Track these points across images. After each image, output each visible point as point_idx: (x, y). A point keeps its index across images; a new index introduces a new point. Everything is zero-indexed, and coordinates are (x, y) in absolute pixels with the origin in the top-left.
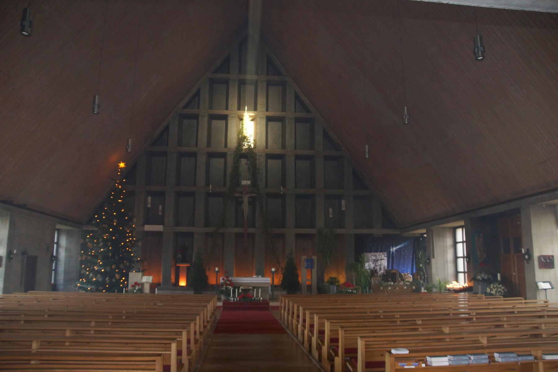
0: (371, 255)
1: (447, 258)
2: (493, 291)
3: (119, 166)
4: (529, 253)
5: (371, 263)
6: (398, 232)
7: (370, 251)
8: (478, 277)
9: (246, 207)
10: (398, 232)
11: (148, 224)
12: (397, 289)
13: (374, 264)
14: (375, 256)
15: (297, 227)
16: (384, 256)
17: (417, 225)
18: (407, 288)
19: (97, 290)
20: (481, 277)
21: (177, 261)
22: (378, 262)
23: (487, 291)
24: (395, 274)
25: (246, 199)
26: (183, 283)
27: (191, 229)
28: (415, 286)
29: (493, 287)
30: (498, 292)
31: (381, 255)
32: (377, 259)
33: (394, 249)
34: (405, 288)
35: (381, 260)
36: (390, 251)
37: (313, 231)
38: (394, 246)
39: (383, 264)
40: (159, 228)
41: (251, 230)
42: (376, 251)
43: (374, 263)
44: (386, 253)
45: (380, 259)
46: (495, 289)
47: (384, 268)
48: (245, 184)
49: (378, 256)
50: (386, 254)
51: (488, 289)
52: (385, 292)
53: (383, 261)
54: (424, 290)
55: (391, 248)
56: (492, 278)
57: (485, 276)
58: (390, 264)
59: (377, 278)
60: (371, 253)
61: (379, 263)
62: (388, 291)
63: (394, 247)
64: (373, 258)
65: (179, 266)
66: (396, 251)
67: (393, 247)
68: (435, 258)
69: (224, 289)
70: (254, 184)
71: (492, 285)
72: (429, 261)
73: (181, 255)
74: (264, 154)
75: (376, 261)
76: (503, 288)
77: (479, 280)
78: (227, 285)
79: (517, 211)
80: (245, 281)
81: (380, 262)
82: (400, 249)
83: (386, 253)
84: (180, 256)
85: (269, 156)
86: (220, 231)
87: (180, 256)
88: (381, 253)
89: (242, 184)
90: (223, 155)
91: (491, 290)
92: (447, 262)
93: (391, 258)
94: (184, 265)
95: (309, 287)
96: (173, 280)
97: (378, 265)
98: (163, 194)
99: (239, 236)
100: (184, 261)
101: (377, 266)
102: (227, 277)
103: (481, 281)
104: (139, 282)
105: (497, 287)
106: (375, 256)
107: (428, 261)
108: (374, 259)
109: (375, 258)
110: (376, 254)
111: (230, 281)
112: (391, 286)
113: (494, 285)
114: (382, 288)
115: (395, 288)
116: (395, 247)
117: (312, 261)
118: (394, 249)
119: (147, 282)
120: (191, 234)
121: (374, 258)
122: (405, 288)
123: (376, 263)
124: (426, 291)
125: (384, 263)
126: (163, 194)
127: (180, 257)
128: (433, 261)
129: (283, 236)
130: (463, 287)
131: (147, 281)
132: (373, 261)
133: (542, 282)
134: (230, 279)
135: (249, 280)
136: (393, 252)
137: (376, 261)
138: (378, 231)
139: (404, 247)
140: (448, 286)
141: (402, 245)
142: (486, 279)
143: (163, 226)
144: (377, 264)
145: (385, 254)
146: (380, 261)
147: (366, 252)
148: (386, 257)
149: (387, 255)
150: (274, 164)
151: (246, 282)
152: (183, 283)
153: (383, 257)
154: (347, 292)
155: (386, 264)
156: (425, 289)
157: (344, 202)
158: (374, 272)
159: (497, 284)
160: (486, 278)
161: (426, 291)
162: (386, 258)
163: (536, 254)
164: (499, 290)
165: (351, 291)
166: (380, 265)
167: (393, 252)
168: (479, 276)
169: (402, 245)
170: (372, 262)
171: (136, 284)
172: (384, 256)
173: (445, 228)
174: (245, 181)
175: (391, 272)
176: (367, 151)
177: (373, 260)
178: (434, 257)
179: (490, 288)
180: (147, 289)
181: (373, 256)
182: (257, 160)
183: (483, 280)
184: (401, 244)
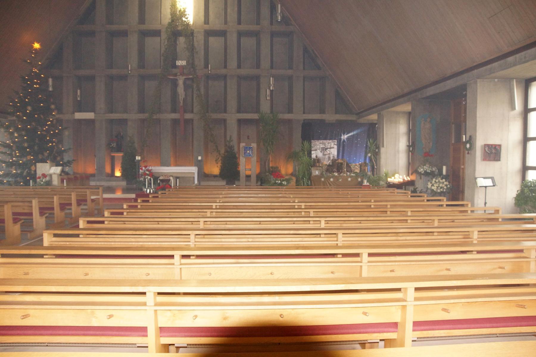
0: (319, 142)
1: (399, 148)
2: (434, 186)
3: (33, 47)
4: (471, 140)
5: (319, 151)
6: (353, 118)
7: (319, 139)
8: (420, 169)
9: (181, 90)
10: (353, 118)
11: (80, 111)
12: (340, 180)
13: (323, 152)
14: (323, 143)
15: (239, 111)
16: (334, 144)
17: (370, 109)
18: (351, 180)
19: (17, 183)
20: (424, 170)
21: (112, 150)
22: (327, 150)
23: (428, 186)
24: (342, 164)
25: (181, 82)
26: (118, 174)
27: (124, 116)
28: (360, 178)
29: (435, 181)
30: (439, 188)
31: (330, 143)
32: (326, 147)
33: (346, 136)
34: (349, 179)
35: (330, 148)
36: (341, 139)
37: (255, 116)
38: (346, 133)
39: (332, 153)
40: (90, 115)
41: (188, 116)
42: (325, 139)
43: (323, 151)
44: (336, 141)
45: (329, 147)
46: (436, 184)
47: (334, 157)
48: (179, 65)
49: (327, 144)
50: (336, 142)
51: (429, 183)
52: (327, 185)
53: (332, 150)
54: (367, 183)
55: (342, 135)
56: (437, 171)
57: (428, 169)
58: (341, 154)
59: (318, 168)
60: (319, 141)
61: (328, 152)
62: (330, 182)
63: (345, 134)
64: (322, 147)
65: (114, 156)
66: (348, 139)
67: (344, 134)
68: (385, 146)
69: (143, 179)
70: (191, 64)
71: (434, 180)
72: (378, 150)
73: (115, 144)
74: (203, 30)
75: (324, 149)
76: (445, 183)
77: (420, 174)
78: (146, 174)
79: (463, 88)
80: (167, 170)
81: (329, 151)
83: (336, 141)
84: (114, 145)
85: (209, 33)
86: (155, 117)
87: (114, 145)
88: (331, 141)
89: (177, 65)
90: (157, 33)
91: (433, 185)
92: (398, 152)
93: (341, 146)
94: (120, 155)
95: (248, 177)
96: (108, 170)
98: (92, 78)
99: (175, 122)
100: (119, 150)
101: (326, 155)
102: (146, 167)
103: (423, 174)
104: (46, 173)
105: (439, 182)
106: (324, 144)
107: (377, 150)
108: (323, 147)
109: (324, 146)
110: (325, 141)
111: (148, 170)
112: (334, 177)
113: (436, 179)
114: (323, 179)
115: (338, 180)
116: (347, 134)
118: (346, 136)
119: (54, 173)
120: (123, 122)
121: (322, 146)
122: (349, 179)
123: (324, 152)
124: (368, 184)
125: (334, 152)
126: (92, 78)
127: (114, 146)
128: (383, 150)
130: (404, 180)
131: (55, 172)
132: (321, 149)
133: (483, 178)
134: (150, 168)
135: (172, 170)
136: (344, 141)
138: (330, 117)
139: (357, 134)
140: (389, 180)
141: (355, 132)
142: (428, 172)
143: (95, 113)
144: (325, 153)
145: (335, 142)
146: (329, 150)
147: (313, 139)
148: (335, 145)
150: (215, 43)
151: (168, 171)
152: (118, 174)
154: (275, 183)
155: (336, 153)
156: (367, 182)
157: (272, 79)
158: (316, 161)
159: (440, 179)
160: (429, 171)
161: (368, 184)
162: (336, 147)
163: (480, 142)
164: (441, 185)
165: (279, 182)
166: (329, 154)
167: (344, 141)
168: (422, 168)
169: (355, 132)
170: (321, 151)
171: (44, 176)
172: (334, 144)
173: (398, 113)
174: (180, 61)
175: (337, 162)
176: (279, 12)
177: (322, 148)
178: (383, 146)
179: (431, 183)
180: (56, 181)
183: (426, 174)
184: (354, 131)
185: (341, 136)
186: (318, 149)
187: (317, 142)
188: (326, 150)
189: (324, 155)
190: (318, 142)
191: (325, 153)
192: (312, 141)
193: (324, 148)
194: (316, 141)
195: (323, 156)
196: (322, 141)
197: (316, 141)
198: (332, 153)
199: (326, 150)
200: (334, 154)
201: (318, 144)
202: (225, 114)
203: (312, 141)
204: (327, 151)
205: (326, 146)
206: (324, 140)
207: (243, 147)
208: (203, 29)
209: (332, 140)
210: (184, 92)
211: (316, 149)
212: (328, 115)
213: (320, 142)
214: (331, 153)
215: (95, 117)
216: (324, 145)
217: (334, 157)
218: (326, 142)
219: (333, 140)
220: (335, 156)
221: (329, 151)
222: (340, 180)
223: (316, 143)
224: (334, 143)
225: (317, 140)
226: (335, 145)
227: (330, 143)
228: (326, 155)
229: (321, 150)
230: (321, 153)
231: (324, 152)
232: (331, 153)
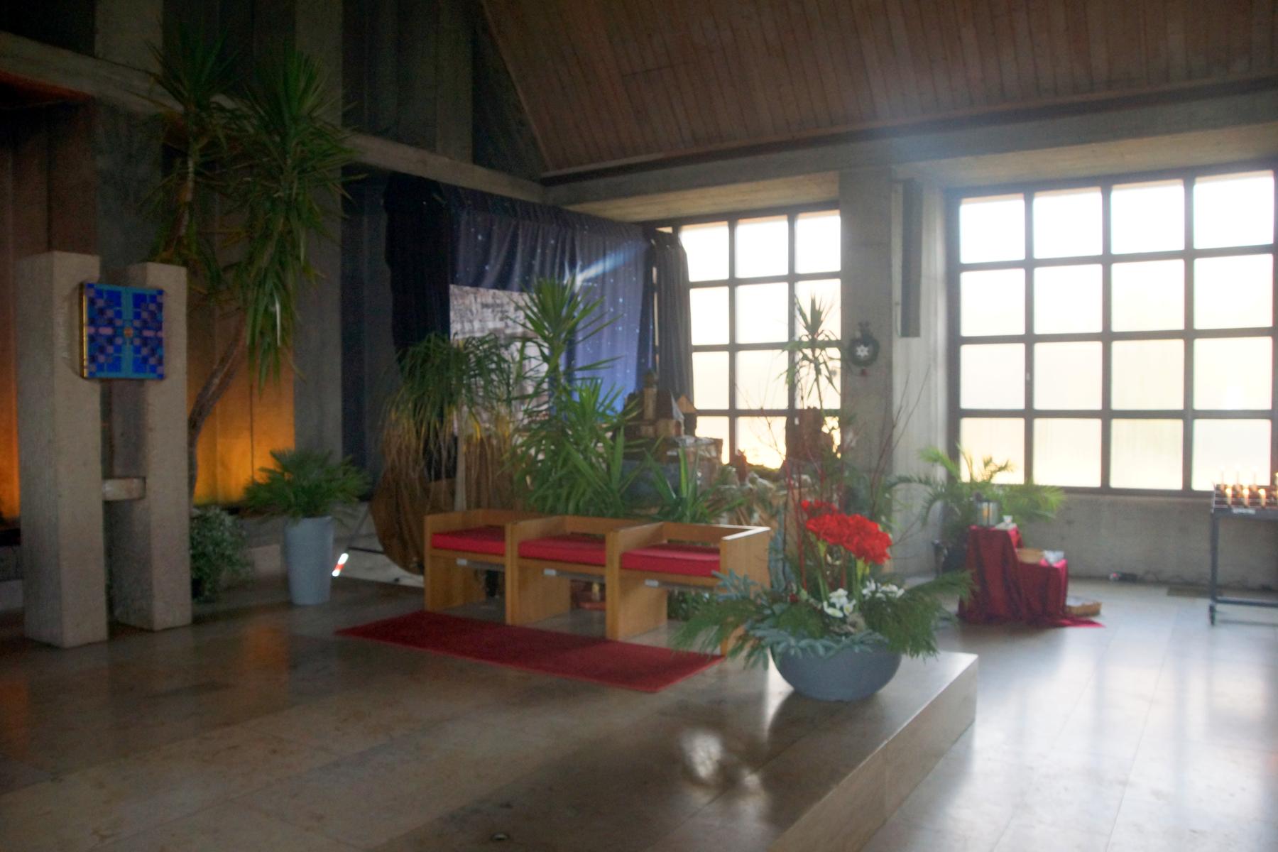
67: (573, 266)
82: (601, 279)
110: (502, 296)
116: (582, 270)
117: (149, 303)
118: (580, 278)
139: (615, 272)
181: (488, 312)
185: (561, 275)
187: (472, 297)
190: (476, 298)
192: (452, 287)
194: (468, 288)
197: (467, 293)
205: (507, 326)
207: (81, 286)
216: (502, 319)
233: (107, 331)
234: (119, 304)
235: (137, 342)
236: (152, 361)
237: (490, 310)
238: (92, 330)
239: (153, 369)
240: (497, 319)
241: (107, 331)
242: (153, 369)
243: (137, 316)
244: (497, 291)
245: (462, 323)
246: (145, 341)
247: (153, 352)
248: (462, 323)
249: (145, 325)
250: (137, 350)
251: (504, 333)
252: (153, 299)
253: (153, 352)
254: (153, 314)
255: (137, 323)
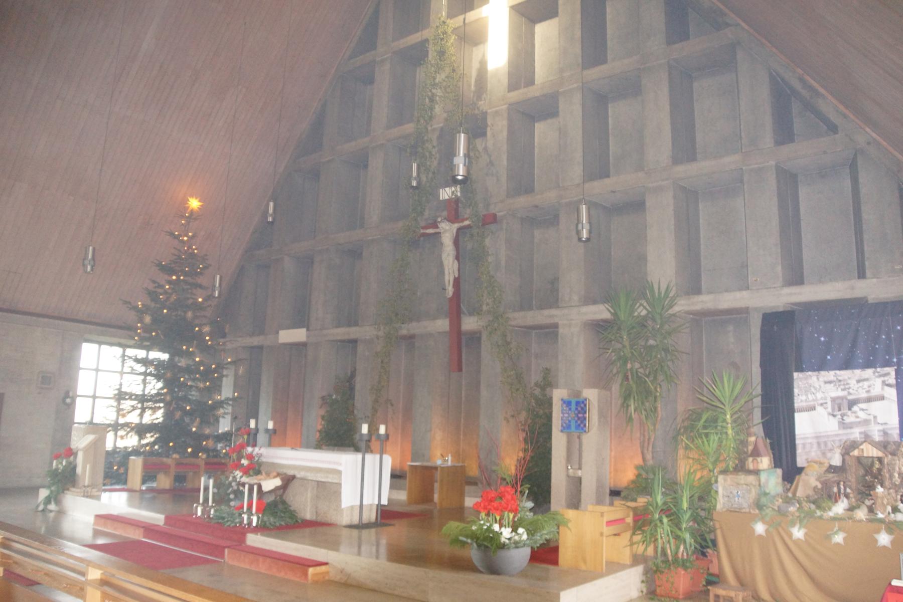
0: (821, 379)
7: (821, 366)
16: (884, 384)
22: (855, 408)
31: (866, 380)
32: (850, 397)
35: (869, 400)
39: (879, 420)
42: (847, 365)
44: (892, 371)
45: (863, 395)
49: (853, 383)
50: (893, 373)
53: (875, 408)
60: (823, 373)
61: (862, 415)
74: (505, 107)
81: (863, 410)
83: (892, 371)
88: (869, 372)
97: (858, 420)
101: (850, 426)
108: (838, 398)
109: (840, 393)
110: (844, 374)
121: (835, 392)
123: (843, 415)
129: (550, 332)
137: (845, 404)
143: (308, 330)
145: (888, 374)
147: (800, 369)
148: (889, 385)
149: (896, 378)
153: (877, 387)
162: (892, 393)
166: (866, 422)
170: (830, 410)
172: (884, 384)
177: (833, 400)
182: (489, 129)
186: (822, 405)
187: (814, 378)
188: (850, 409)
189: (843, 425)
190: (818, 379)
191: (847, 420)
192: (796, 375)
193: (842, 398)
194: (810, 373)
195: (841, 432)
196: (832, 373)
197: (811, 376)
198: (875, 417)
199: (850, 409)
200: (885, 424)
201: (817, 386)
202: (553, 312)
203: (796, 375)
204: (855, 412)
205: (849, 394)
206: (840, 369)
208: (505, 104)
209: (875, 368)
210: (456, 262)
211: (812, 403)
212: (875, 280)
213: (826, 379)
214: (871, 417)
215: (308, 337)
216: (843, 390)
217: (885, 433)
218: (849, 378)
219: (878, 370)
220: (889, 432)
221: (863, 410)
222: (839, 538)
223: (810, 381)
224: (886, 378)
225: (814, 370)
226: (886, 388)
227: (866, 380)
228: (850, 426)
229: (833, 409)
230: (831, 417)
231: (843, 415)
232: (871, 417)
233: (580, 415)
234: (571, 405)
235: (576, 419)
236: (582, 426)
237: (832, 385)
238: (585, 415)
239: (582, 429)
240: (840, 389)
241: (580, 415)
242: (582, 429)
243: (577, 409)
244: (838, 372)
245: (807, 395)
246: (579, 418)
247: (582, 422)
248: (807, 395)
249: (579, 412)
250: (576, 422)
251: (847, 399)
252: (583, 402)
253: (582, 422)
254: (582, 408)
255: (576, 412)
